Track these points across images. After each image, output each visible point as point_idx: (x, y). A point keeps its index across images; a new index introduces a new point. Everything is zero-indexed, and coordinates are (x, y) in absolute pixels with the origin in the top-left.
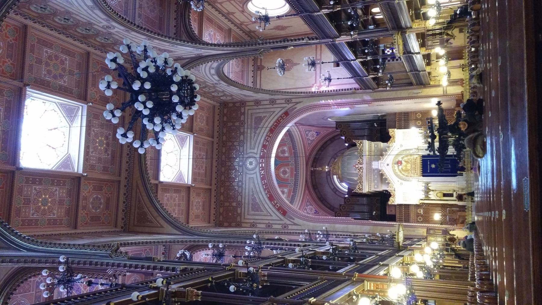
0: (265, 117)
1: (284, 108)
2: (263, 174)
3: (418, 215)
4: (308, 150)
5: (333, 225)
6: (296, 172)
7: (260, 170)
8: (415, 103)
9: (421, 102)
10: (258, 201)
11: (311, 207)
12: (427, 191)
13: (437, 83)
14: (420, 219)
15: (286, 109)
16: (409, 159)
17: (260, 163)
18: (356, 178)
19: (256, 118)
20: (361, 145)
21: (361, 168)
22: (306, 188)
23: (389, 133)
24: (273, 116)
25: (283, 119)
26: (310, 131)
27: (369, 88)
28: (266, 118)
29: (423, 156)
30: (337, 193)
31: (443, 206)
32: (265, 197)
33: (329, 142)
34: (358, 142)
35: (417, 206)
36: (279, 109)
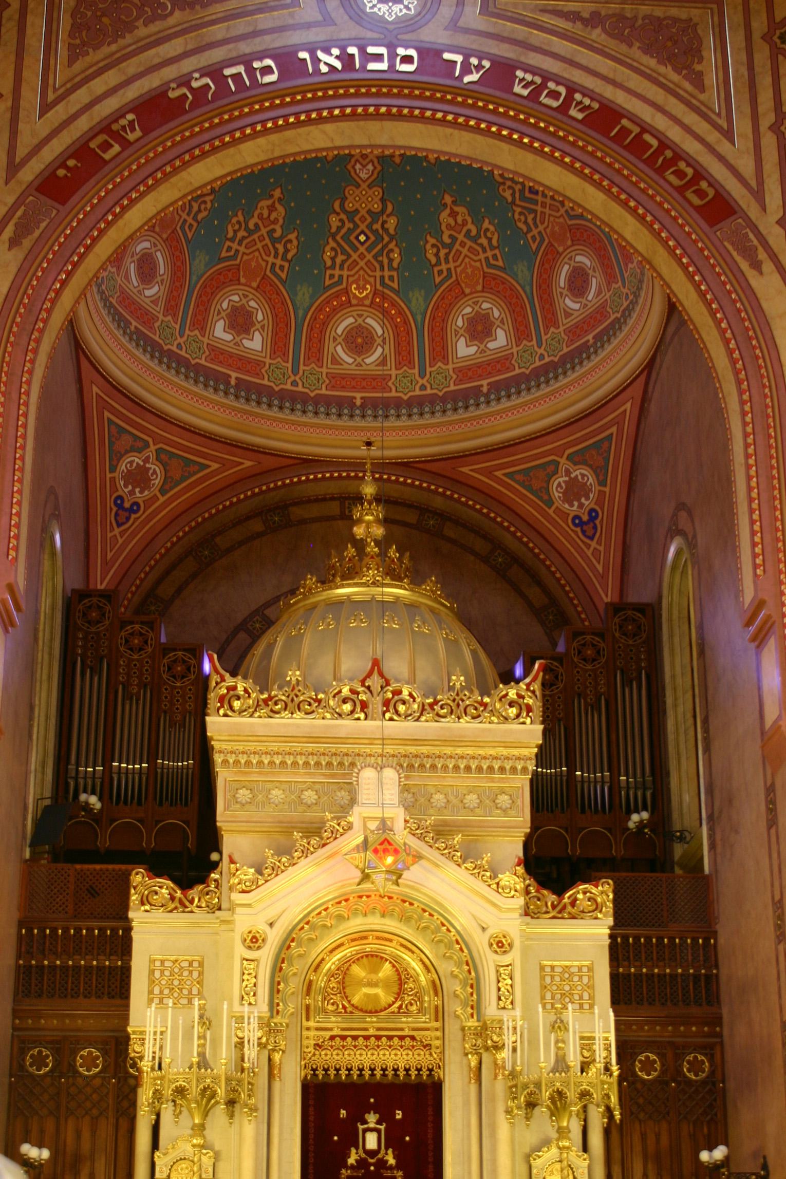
0: (698, 81)
1: (759, 195)
2: (316, 61)
4: (489, 472)
6: (363, 406)
7: (343, 49)
10: (142, 31)
11: (157, 482)
15: (753, 211)
16: (419, 997)
17: (393, 56)
19: (689, 26)
22: (270, 462)
24: (702, 127)
25: (681, 190)
26: (600, 472)
28: (687, 86)
30: (242, 635)
32: (170, 73)
33: (534, 593)
36: (747, 166)
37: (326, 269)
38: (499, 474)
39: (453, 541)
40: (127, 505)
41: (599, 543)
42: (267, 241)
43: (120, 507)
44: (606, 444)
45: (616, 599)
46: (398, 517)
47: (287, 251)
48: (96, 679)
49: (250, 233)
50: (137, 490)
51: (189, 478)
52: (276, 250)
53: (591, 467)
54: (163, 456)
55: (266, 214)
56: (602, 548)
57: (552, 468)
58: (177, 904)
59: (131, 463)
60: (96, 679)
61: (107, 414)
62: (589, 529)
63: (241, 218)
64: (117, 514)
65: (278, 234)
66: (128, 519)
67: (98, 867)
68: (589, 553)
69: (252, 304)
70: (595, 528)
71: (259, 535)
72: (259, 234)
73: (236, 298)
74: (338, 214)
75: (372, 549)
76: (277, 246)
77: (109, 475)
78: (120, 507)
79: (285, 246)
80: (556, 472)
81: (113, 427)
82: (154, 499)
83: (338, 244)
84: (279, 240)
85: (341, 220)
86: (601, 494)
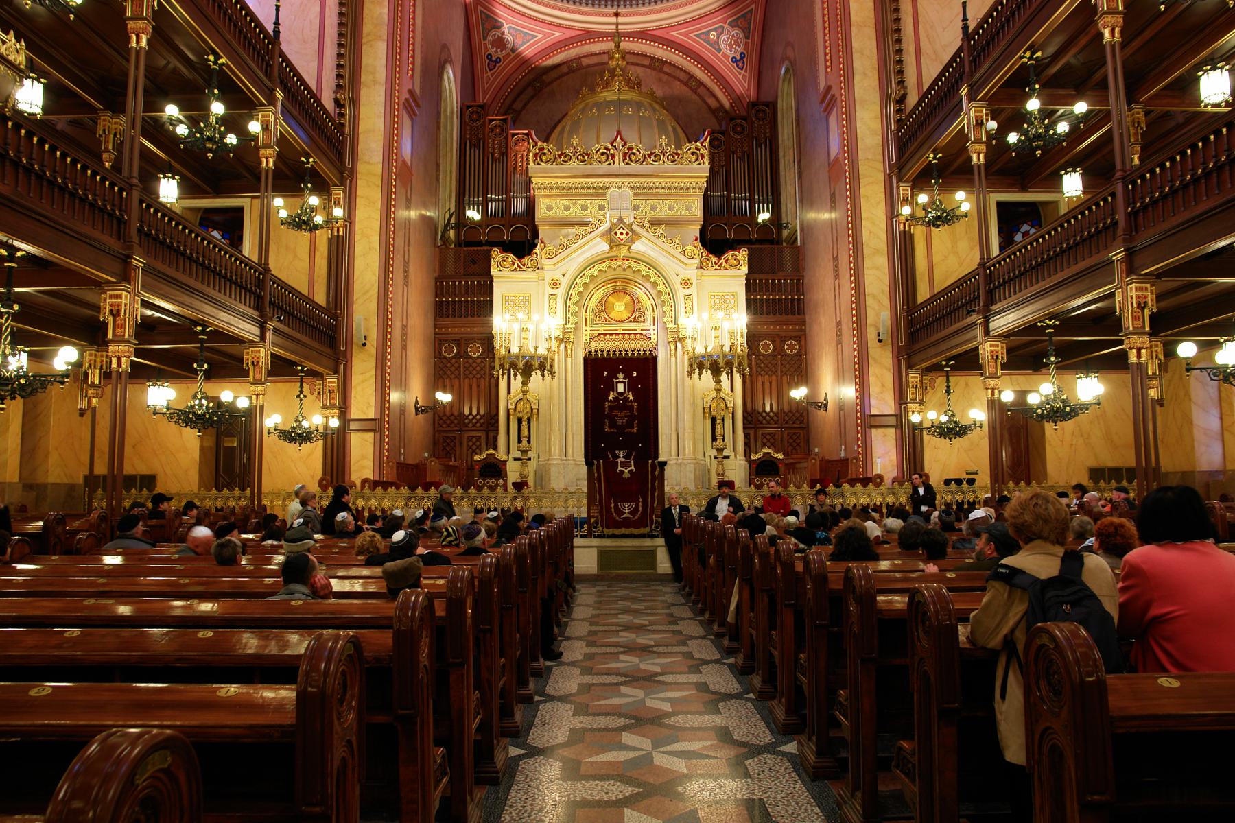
3: (461, 343)
4: (686, 35)
5: (383, 32)
8: (839, 324)
9: (839, 342)
12: (527, 366)
13: (911, 394)
14: (450, 350)
18: (574, 141)
20: (693, 158)
21: (613, 156)
22: (572, 33)
23: (734, 249)
27: (901, 151)
29: (655, 359)
31: (491, 421)
34: (703, 146)
35: (488, 341)
38: (692, 35)
39: (668, 74)
40: (494, 59)
41: (746, 72)
43: (490, 60)
44: (750, 14)
45: (753, 95)
46: (639, 62)
48: (477, 151)
50: (499, 50)
51: (526, 43)
53: (741, 28)
54: (511, 31)
56: (747, 75)
57: (720, 30)
58: (516, 266)
59: (495, 35)
60: (477, 151)
61: (479, 7)
62: (741, 65)
64: (488, 64)
66: (495, 67)
67: (475, 248)
68: (740, 77)
70: (743, 63)
71: (566, 74)
75: (618, 72)
77: (483, 42)
78: (490, 60)
80: (722, 33)
81: (483, 15)
82: (509, 55)
86: (747, 44)
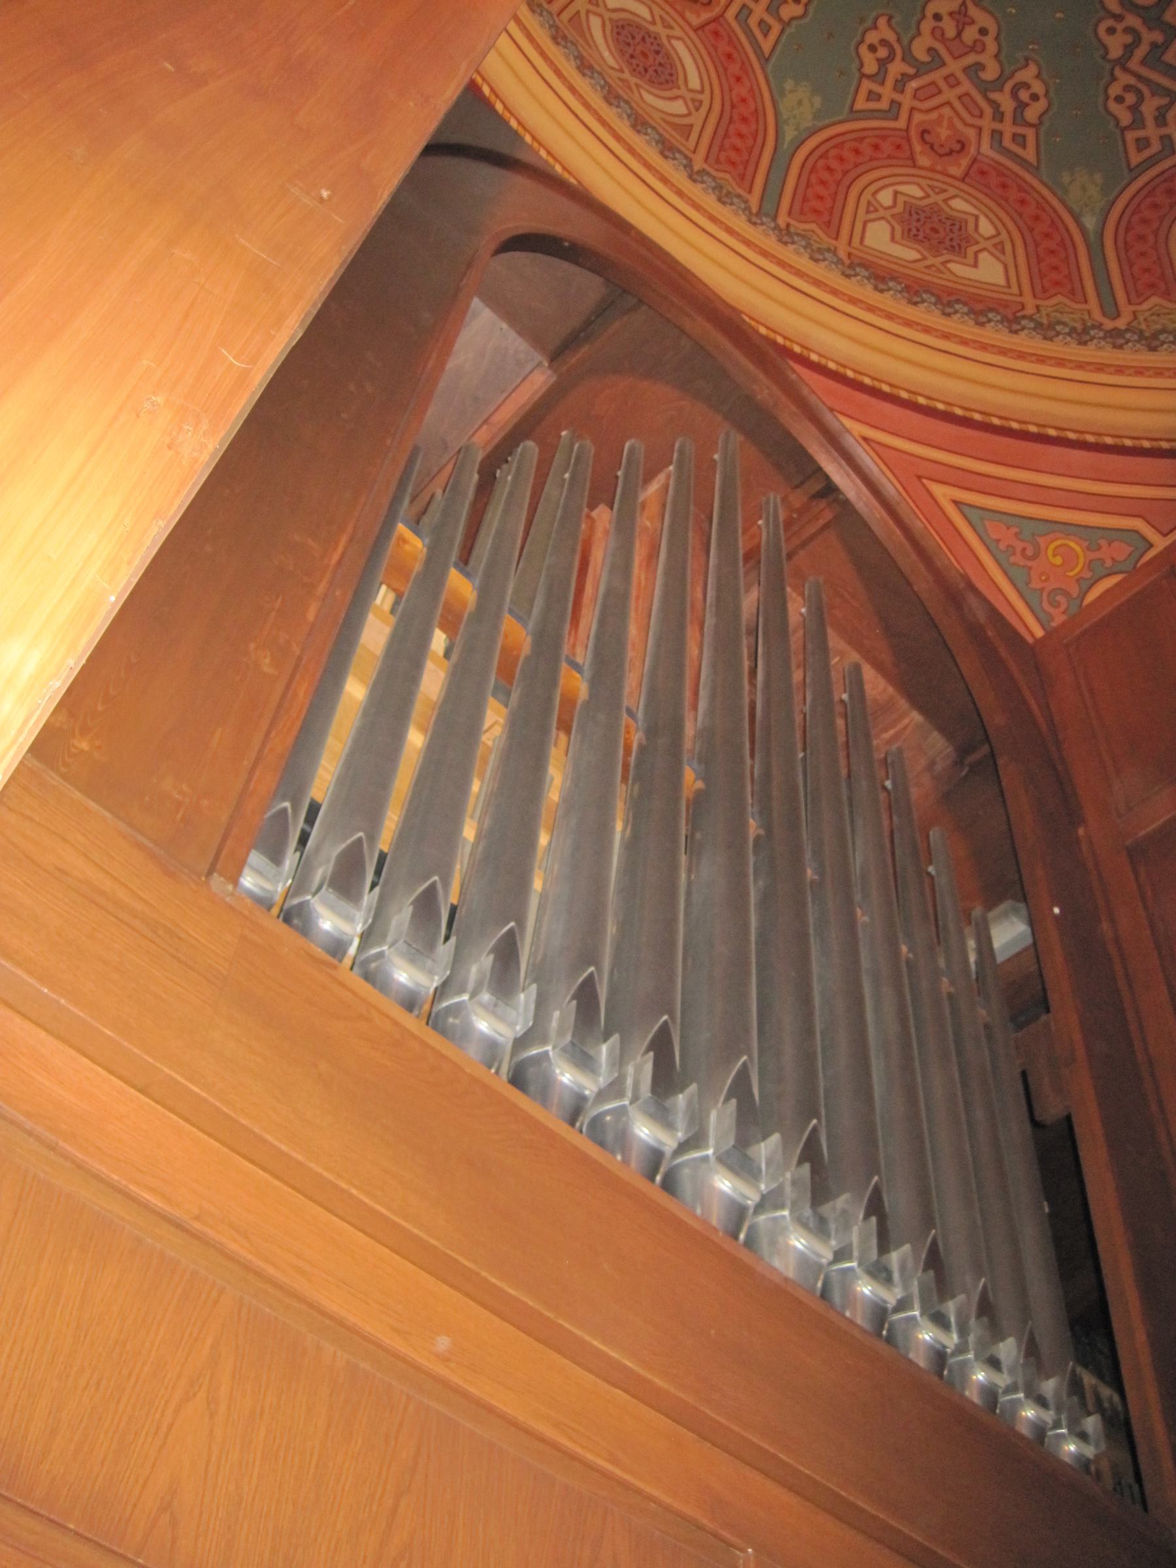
37: (1123, 130)
42: (966, 86)
47: (1021, 106)
49: (921, 69)
52: (996, 105)
55: (951, 32)
63: (891, 37)
65: (990, 73)
69: (958, 204)
72: (944, 71)
73: (914, 191)
74: (1119, 18)
76: (995, 96)
79: (1014, 94)
83: (1139, 77)
84: (998, 84)
85: (1128, 30)
